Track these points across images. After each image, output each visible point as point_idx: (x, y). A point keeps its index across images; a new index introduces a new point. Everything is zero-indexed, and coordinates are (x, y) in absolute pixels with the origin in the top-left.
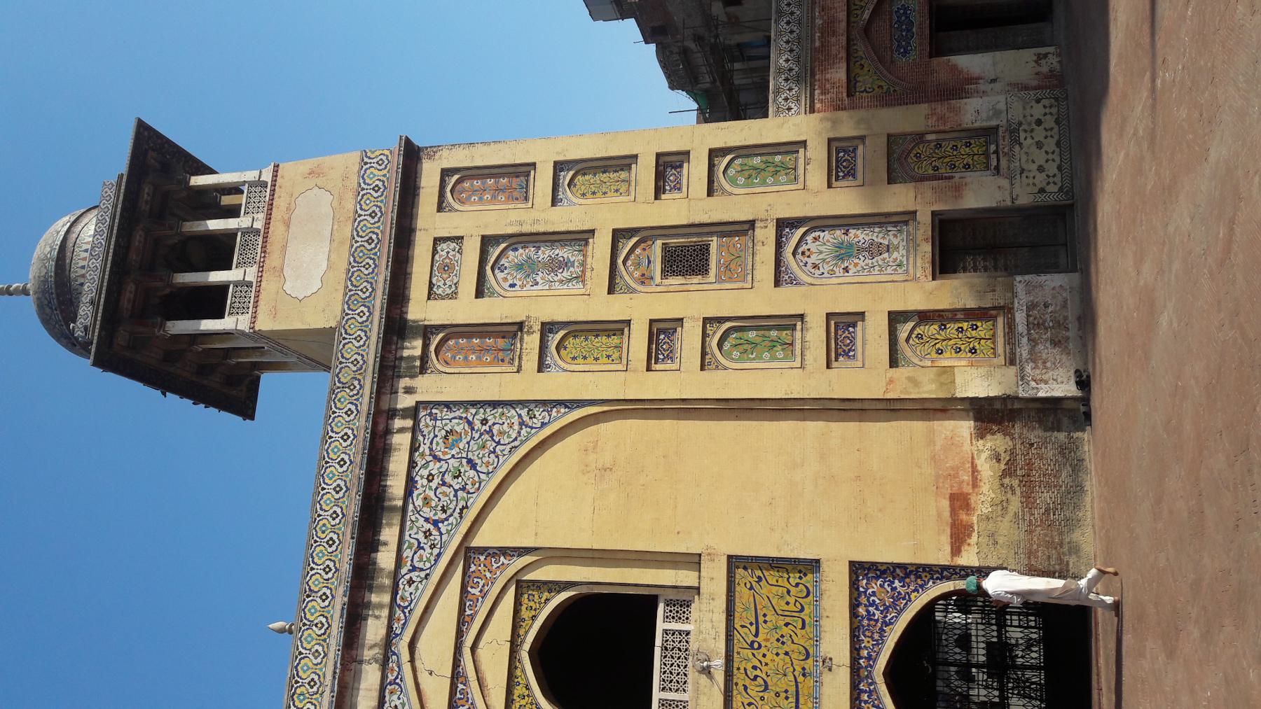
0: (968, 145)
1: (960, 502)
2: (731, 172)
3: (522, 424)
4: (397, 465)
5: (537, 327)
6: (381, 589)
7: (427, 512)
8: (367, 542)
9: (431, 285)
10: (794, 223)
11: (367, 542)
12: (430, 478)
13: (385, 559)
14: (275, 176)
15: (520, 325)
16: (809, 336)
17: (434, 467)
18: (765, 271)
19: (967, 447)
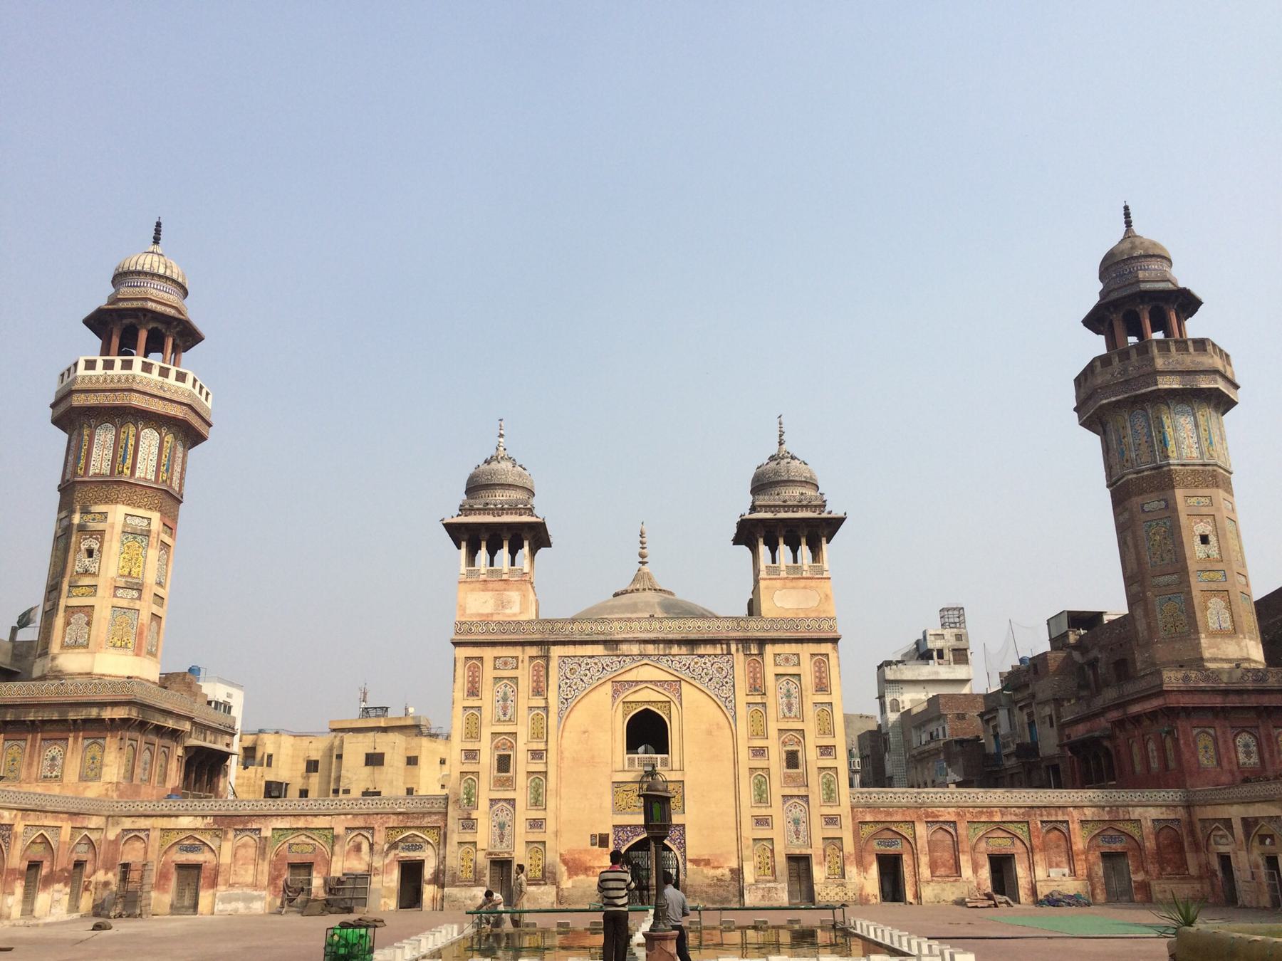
0: (838, 868)
1: (707, 863)
2: (828, 776)
3: (727, 698)
4: (709, 650)
5: (764, 701)
6: (665, 648)
7: (692, 664)
8: (680, 642)
9: (779, 654)
10: (807, 802)
11: (680, 642)
12: (705, 663)
13: (675, 649)
14: (825, 578)
15: (765, 694)
16: (764, 809)
17: (709, 664)
18: (788, 792)
19: (726, 865)
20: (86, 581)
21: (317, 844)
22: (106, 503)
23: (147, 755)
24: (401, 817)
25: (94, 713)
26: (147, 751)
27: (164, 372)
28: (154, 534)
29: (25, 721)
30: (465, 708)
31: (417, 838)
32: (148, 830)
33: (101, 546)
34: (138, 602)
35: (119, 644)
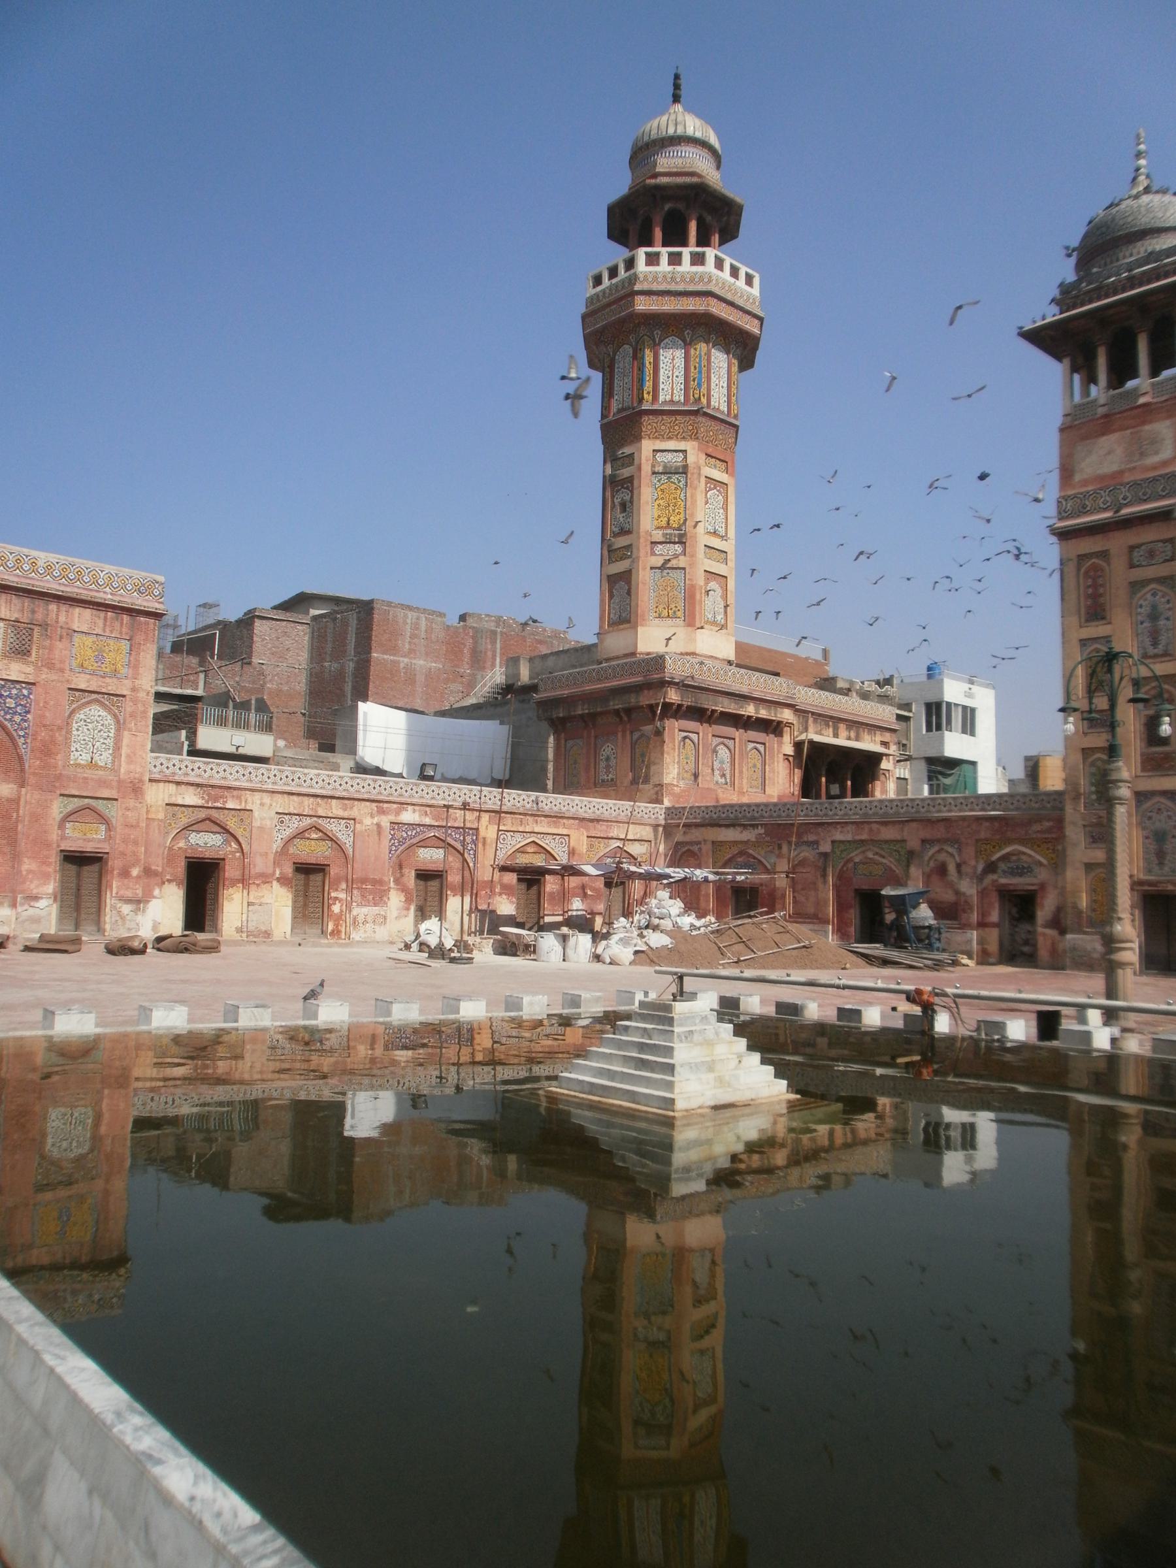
20: (621, 542)
21: (888, 864)
22: (632, 442)
23: (723, 752)
24: (996, 824)
25: (633, 700)
26: (722, 746)
27: (675, 259)
28: (690, 470)
29: (575, 717)
30: (1083, 642)
31: (1024, 857)
32: (698, 843)
33: (632, 492)
34: (682, 558)
35: (665, 613)
